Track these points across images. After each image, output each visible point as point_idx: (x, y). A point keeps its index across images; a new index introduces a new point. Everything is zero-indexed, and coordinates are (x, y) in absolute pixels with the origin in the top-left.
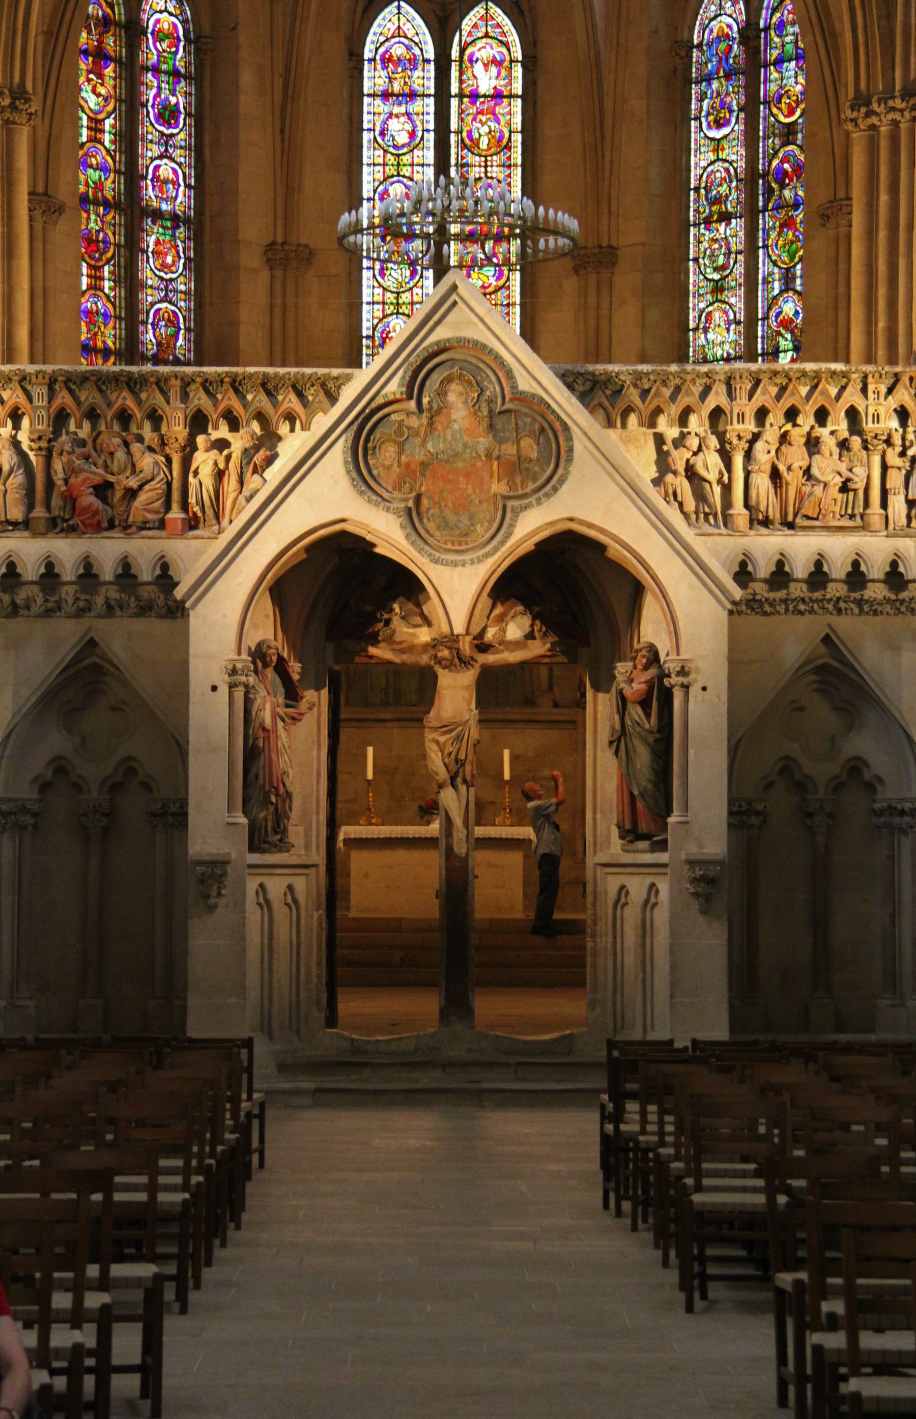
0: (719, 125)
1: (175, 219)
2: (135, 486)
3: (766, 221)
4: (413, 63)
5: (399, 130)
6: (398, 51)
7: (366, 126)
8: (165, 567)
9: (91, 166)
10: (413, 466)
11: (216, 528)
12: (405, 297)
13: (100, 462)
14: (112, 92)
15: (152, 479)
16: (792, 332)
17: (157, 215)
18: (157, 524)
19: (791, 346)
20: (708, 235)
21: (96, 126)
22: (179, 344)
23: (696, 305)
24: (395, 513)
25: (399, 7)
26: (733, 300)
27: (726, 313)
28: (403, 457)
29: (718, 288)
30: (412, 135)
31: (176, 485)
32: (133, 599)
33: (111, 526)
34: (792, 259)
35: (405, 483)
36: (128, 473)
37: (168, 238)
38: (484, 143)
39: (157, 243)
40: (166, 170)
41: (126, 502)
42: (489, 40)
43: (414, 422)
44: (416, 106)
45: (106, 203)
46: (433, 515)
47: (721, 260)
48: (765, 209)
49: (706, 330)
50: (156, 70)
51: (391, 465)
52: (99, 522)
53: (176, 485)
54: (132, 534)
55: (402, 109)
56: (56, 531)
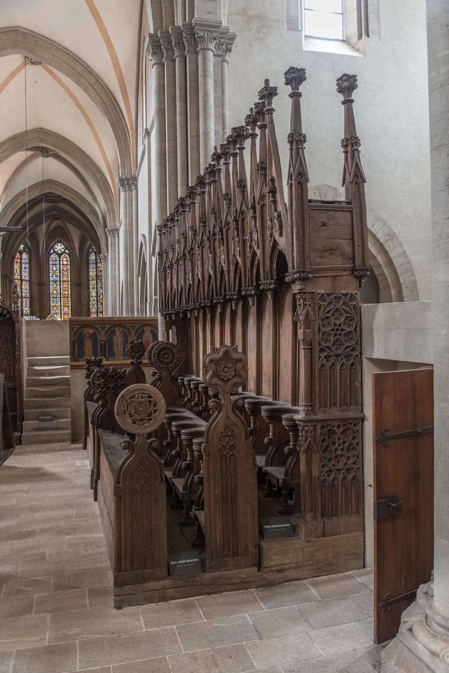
0: (93, 269)
1: (27, 281)
3: (99, 281)
4: (56, 261)
5: (54, 269)
6: (54, 259)
17: (24, 280)
23: (91, 290)
29: (93, 288)
40: (25, 275)
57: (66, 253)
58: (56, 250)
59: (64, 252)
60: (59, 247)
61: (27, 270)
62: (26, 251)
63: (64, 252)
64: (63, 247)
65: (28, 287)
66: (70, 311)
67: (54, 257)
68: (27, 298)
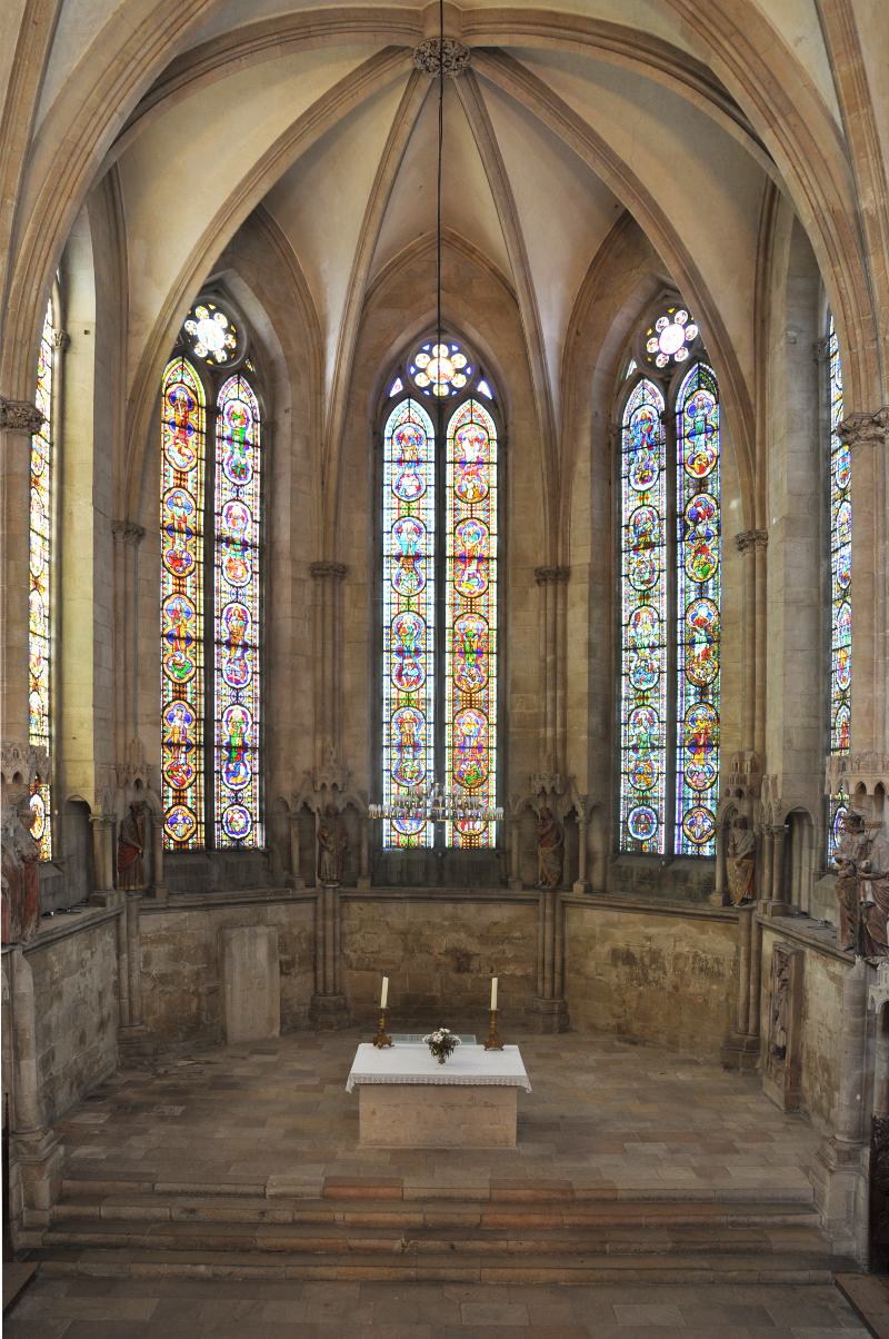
0: (643, 480)
1: (245, 545)
5: (409, 486)
7: (385, 482)
9: (177, 505)
12: (413, 600)
14: (195, 453)
16: (706, 630)
17: (230, 541)
19: (704, 639)
20: (636, 559)
21: (181, 475)
22: (246, 633)
23: (627, 608)
25: (409, 403)
26: (657, 605)
27: (651, 614)
29: (645, 596)
30: (419, 488)
34: (705, 576)
37: (238, 557)
38: (470, 495)
39: (230, 560)
42: (473, 425)
44: (421, 469)
45: (189, 533)
47: (647, 577)
48: (682, 539)
49: (635, 626)
50: (230, 440)
55: (412, 471)
57: (480, 398)
58: (421, 381)
59: (469, 393)
60: (441, 367)
61: (253, 486)
62: (241, 372)
63: (469, 393)
64: (460, 360)
65: (253, 589)
66: (493, 731)
67: (408, 418)
68: (245, 647)
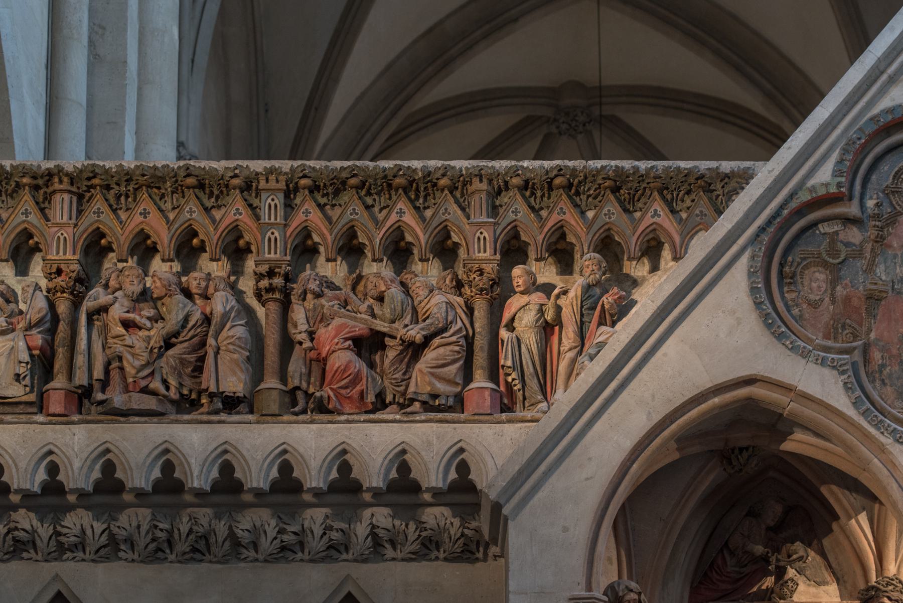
2: (419, 338)
8: (463, 468)
10: (855, 302)
11: (545, 404)
13: (364, 307)
15: (444, 329)
18: (451, 401)
24: (834, 367)
28: (839, 288)
31: (481, 342)
32: (412, 526)
33: (381, 404)
35: (844, 327)
36: (407, 320)
41: (404, 366)
43: (854, 235)
46: (890, 375)
51: (822, 300)
52: (362, 395)
53: (481, 342)
54: (412, 413)
56: (296, 409)
